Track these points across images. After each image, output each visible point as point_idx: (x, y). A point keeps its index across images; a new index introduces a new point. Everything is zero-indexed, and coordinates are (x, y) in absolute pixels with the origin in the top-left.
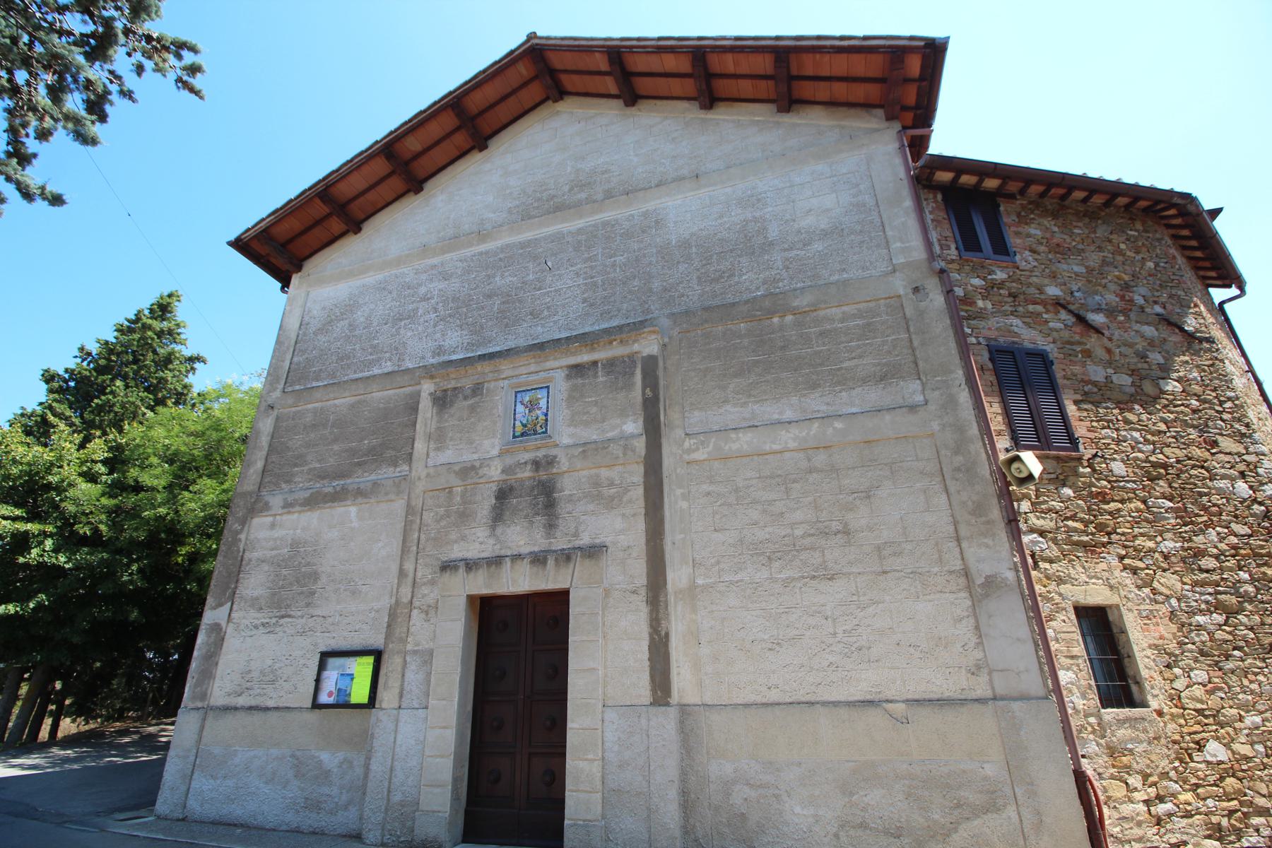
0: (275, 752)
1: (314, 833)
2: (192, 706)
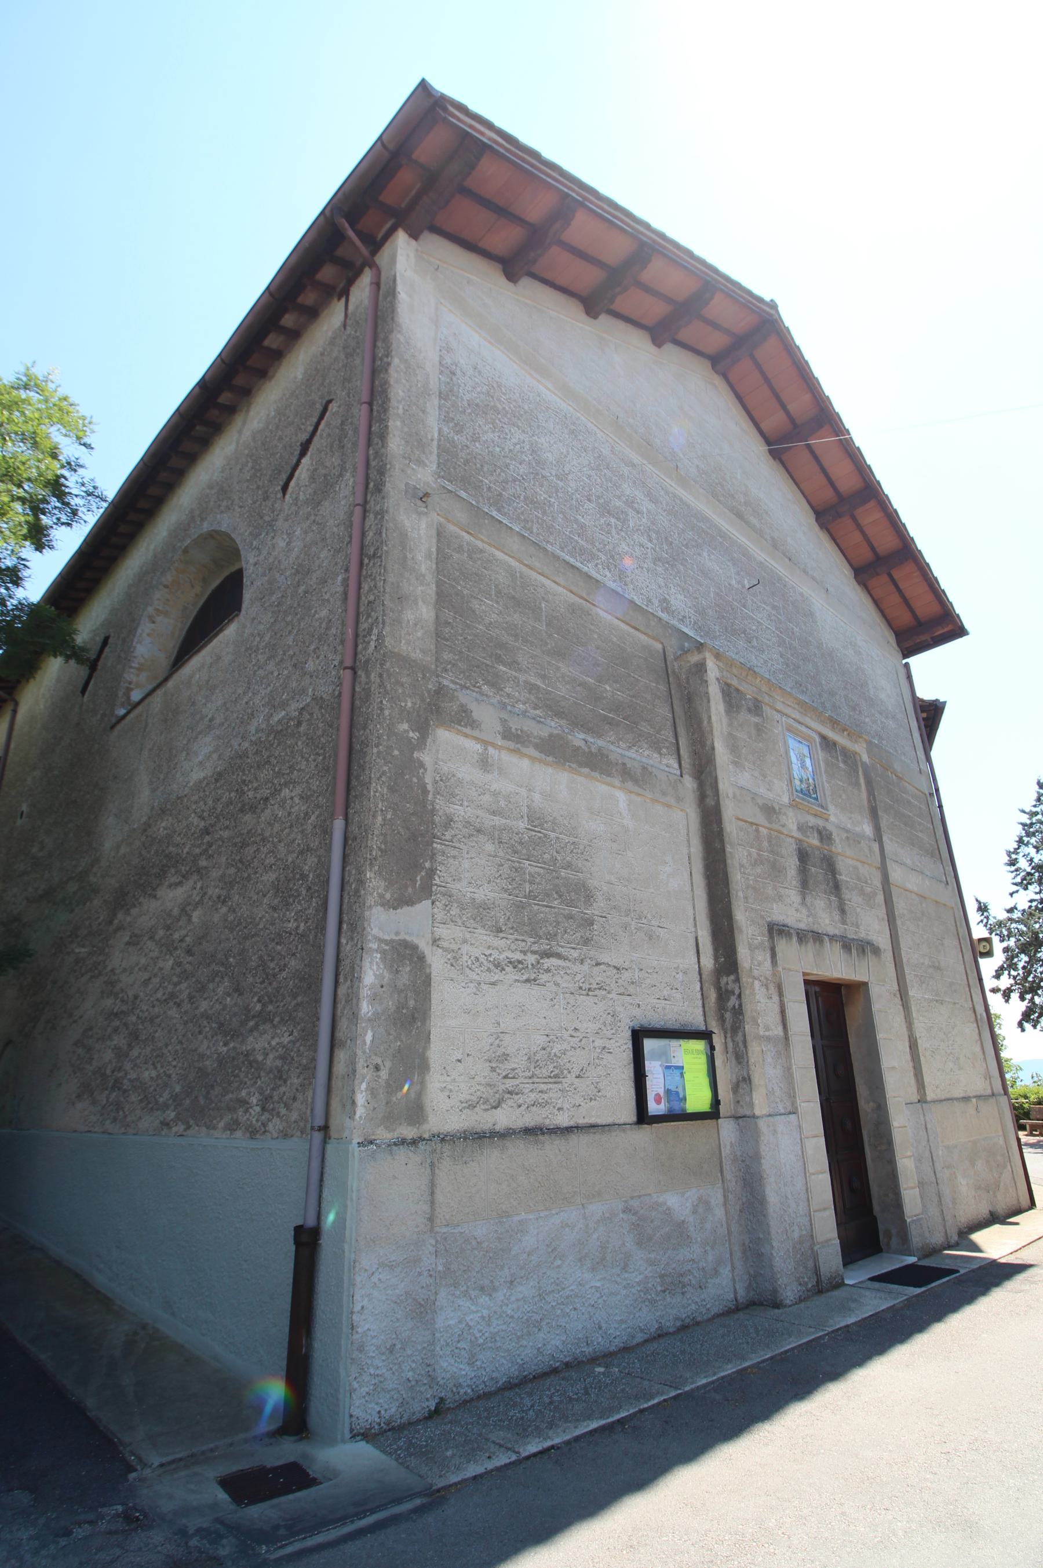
0: (596, 1209)
1: (684, 1328)
2: (384, 1135)
